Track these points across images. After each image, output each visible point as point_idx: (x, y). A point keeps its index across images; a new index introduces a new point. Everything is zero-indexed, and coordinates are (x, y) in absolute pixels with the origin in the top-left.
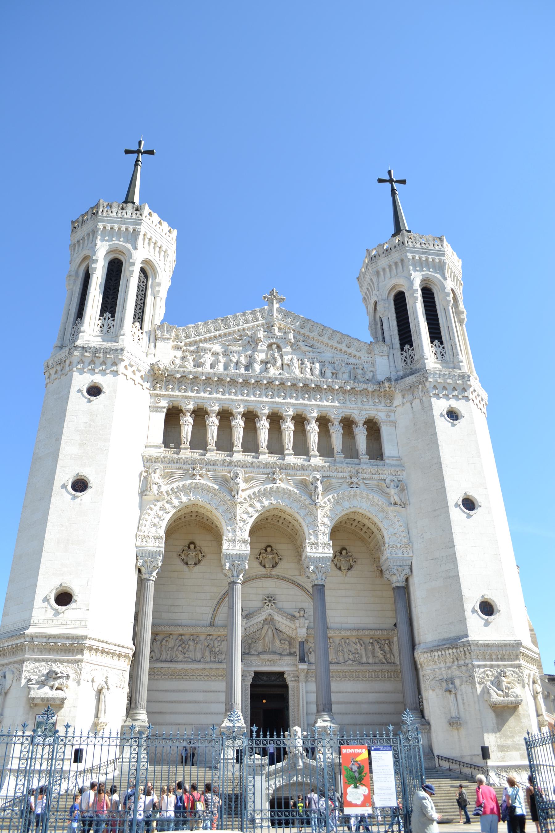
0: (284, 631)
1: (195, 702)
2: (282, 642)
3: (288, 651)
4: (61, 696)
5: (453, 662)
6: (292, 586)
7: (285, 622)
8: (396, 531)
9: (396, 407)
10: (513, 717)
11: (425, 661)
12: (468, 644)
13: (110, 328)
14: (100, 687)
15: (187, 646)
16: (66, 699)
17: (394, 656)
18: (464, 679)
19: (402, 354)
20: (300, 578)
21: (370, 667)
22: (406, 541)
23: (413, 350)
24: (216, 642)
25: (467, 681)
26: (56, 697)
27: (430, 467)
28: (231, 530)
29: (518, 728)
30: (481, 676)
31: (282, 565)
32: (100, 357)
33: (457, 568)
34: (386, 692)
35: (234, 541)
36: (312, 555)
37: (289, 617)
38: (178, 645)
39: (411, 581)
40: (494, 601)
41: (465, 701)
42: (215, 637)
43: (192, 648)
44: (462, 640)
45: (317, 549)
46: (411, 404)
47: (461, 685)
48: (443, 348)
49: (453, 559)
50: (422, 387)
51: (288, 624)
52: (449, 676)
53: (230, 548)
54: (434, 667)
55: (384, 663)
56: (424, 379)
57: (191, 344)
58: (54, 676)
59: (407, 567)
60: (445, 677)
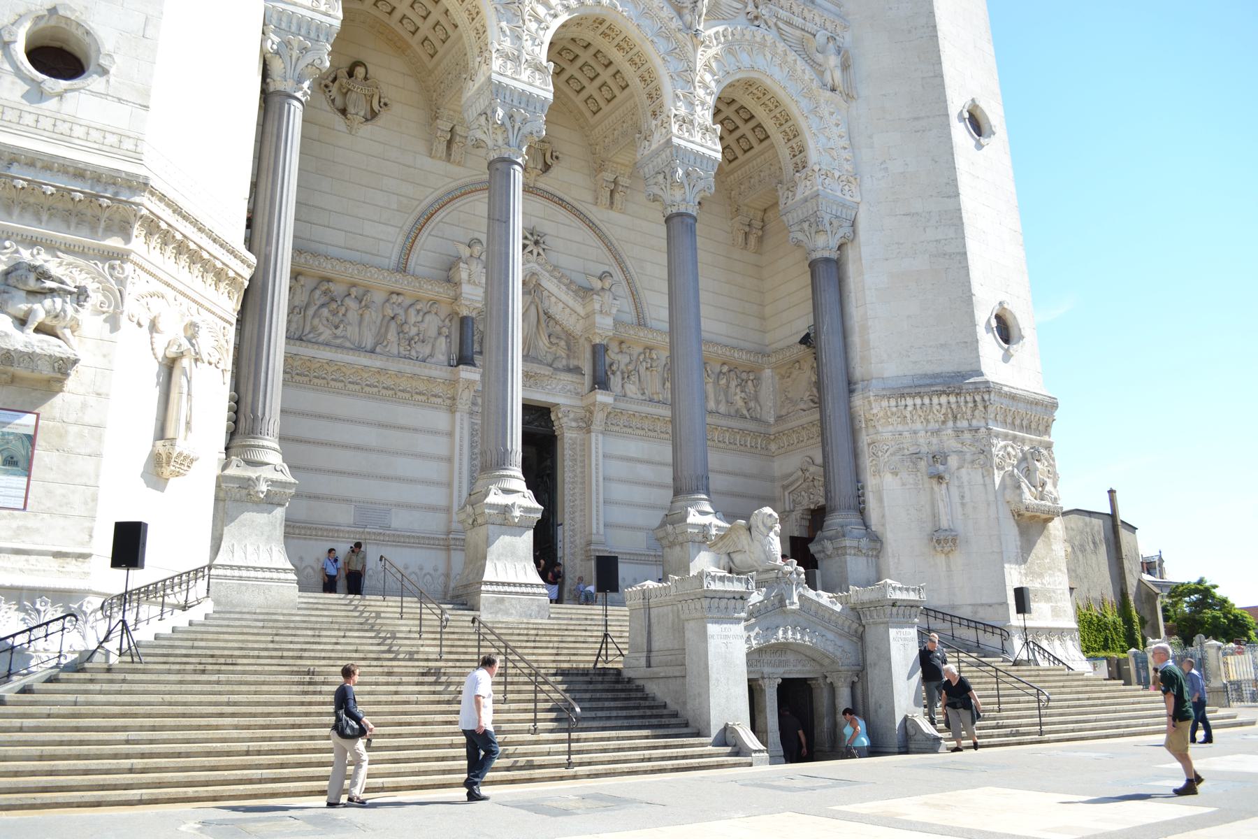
0: (558, 317)
1: (358, 448)
2: (554, 340)
3: (564, 362)
5: (944, 422)
6: (578, 222)
7: (564, 297)
10: (1042, 538)
11: (881, 414)
12: (988, 387)
14: (172, 352)
15: (343, 310)
16: (75, 362)
17: (760, 406)
18: (968, 457)
20: (594, 209)
21: (724, 422)
22: (850, 170)
24: (412, 311)
25: (973, 462)
26: (38, 351)
27: (910, 32)
28: (508, 32)
30: (1001, 453)
31: (556, 171)
33: (964, 238)
34: (745, 476)
35: (516, 59)
36: (683, 143)
37: (573, 287)
38: (318, 303)
39: (850, 253)
40: (1015, 318)
41: (967, 499)
42: (408, 302)
43: (353, 316)
44: (972, 380)
45: (691, 135)
47: (959, 468)
49: (955, 220)
51: (571, 302)
52: (934, 448)
53: (509, 73)
54: (900, 428)
55: (746, 418)
58: (32, 284)
59: (848, 224)
60: (924, 449)
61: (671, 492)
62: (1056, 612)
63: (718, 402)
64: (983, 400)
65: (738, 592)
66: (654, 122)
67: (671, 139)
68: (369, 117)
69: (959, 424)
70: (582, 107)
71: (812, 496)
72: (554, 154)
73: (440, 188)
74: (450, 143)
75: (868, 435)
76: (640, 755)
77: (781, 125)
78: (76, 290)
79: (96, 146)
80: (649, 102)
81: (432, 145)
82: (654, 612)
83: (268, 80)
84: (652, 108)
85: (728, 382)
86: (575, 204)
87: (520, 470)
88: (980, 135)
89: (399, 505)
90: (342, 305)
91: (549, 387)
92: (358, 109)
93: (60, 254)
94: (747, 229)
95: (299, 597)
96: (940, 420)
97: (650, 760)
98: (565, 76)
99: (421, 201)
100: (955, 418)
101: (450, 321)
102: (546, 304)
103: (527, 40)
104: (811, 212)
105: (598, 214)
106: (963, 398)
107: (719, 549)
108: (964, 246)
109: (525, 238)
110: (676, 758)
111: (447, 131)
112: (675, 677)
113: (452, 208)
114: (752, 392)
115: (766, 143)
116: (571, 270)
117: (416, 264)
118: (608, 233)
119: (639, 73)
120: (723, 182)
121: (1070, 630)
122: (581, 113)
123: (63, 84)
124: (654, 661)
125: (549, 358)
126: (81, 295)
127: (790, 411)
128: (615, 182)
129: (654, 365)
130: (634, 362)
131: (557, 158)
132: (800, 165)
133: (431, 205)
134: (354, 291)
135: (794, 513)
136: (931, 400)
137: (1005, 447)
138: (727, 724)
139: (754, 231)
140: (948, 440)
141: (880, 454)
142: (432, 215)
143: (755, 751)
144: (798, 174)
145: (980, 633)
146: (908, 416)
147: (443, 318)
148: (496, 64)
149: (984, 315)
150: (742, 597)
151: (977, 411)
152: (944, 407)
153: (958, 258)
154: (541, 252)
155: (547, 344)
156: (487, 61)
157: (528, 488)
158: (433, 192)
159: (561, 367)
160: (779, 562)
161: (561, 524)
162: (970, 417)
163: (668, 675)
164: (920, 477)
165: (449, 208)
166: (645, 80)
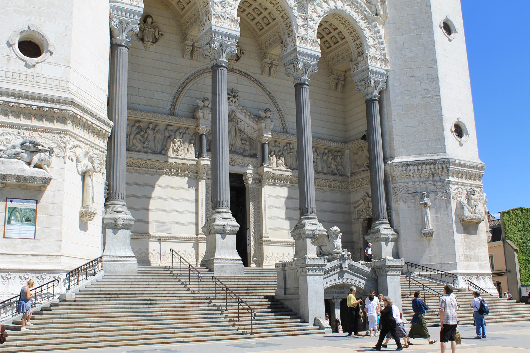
0: (245, 131)
2: (243, 142)
3: (249, 152)
6: (253, 84)
8: (375, 43)
14: (85, 169)
15: (146, 135)
16: (51, 179)
17: (344, 168)
26: (37, 176)
29: (478, 242)
30: (455, 192)
38: (135, 132)
39: (385, 95)
40: (465, 125)
42: (175, 129)
49: (435, 79)
53: (219, 25)
54: (408, 180)
55: (336, 175)
58: (33, 149)
61: (298, 212)
62: (481, 266)
63: (323, 168)
64: (447, 167)
65: (320, 264)
66: (288, 39)
67: (296, 48)
69: (435, 178)
70: (255, 27)
71: (368, 212)
72: (242, 51)
73: (188, 73)
74: (192, 52)
75: (393, 184)
76: (280, 329)
77: (351, 33)
78: (49, 149)
79: (50, 86)
81: (184, 52)
82: (287, 272)
83: (113, 39)
84: (287, 31)
85: (328, 157)
87: (229, 208)
89: (175, 223)
90: (146, 133)
91: (241, 165)
92: (149, 39)
93: (40, 133)
94: (337, 81)
95: (138, 268)
96: (426, 176)
97: (284, 331)
99: (180, 80)
102: (239, 124)
103: (227, 7)
104: (365, 77)
105: (263, 79)
106: (437, 166)
107: (316, 244)
108: (439, 92)
109: (229, 94)
110: (294, 331)
111: (190, 46)
112: (295, 299)
113: (194, 82)
114: (340, 162)
115: (344, 40)
116: (251, 108)
117: (179, 111)
118: (268, 88)
119: (281, 15)
120: (324, 58)
121: (488, 274)
122: (254, 29)
124: (287, 292)
125: (242, 151)
126: (51, 151)
127: (358, 171)
128: (271, 63)
130: (282, 151)
131: (243, 53)
132: (360, 53)
134: (151, 126)
135: (360, 220)
136: (422, 167)
137: (458, 188)
138: (316, 318)
140: (430, 186)
141: (398, 193)
142: (185, 86)
143: (326, 328)
144: (359, 57)
145: (443, 276)
146: (411, 175)
147: (191, 135)
148: (213, 21)
150: (322, 266)
151: (444, 172)
152: (428, 171)
153: (436, 97)
154: (236, 100)
155: (240, 143)
156: (210, 19)
157: (233, 217)
158: (185, 75)
159: (247, 154)
160: (341, 250)
161: (249, 229)
163: (292, 298)
164: (417, 204)
165: (193, 82)
166: (284, 18)
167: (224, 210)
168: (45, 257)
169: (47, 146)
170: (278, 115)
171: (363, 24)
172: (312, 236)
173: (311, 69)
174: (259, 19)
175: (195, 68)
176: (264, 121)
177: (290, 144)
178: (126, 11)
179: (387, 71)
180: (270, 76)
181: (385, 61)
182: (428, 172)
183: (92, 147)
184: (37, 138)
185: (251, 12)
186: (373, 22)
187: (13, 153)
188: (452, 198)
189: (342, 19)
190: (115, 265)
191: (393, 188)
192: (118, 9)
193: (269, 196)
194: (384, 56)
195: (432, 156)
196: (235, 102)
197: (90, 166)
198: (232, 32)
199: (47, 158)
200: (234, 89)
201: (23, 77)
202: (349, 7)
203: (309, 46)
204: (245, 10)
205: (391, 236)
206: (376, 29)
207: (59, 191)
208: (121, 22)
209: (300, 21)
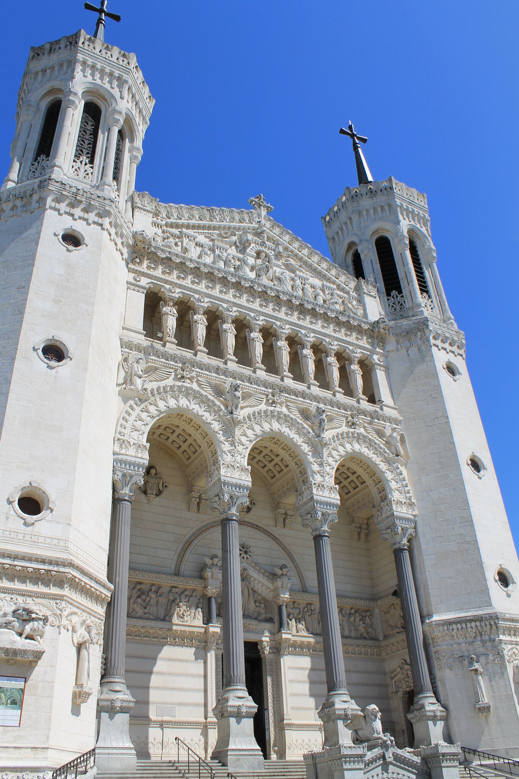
0: (259, 591)
2: (257, 604)
3: (264, 616)
4: (35, 649)
5: (475, 637)
6: (266, 538)
8: (399, 486)
9: (388, 352)
13: (87, 174)
14: (81, 640)
16: (43, 652)
19: (388, 300)
23: (402, 297)
26: (28, 648)
30: (509, 653)
32: (81, 202)
38: (136, 596)
39: (415, 543)
40: (509, 572)
42: (181, 591)
46: (407, 351)
48: (432, 302)
50: (421, 336)
53: (229, 475)
54: (451, 642)
56: (424, 327)
57: (171, 226)
58: (26, 617)
61: (325, 687)
63: (350, 631)
66: (304, 487)
68: (158, 494)
69: (483, 638)
70: (266, 474)
71: (407, 683)
74: (199, 504)
75: (434, 647)
78: (43, 618)
79: (49, 546)
80: (300, 475)
81: (190, 505)
83: (115, 493)
84: (302, 478)
85: (355, 619)
86: (265, 527)
88: (479, 471)
89: (180, 704)
90: (148, 596)
95: (137, 763)
96: (473, 636)
98: (256, 460)
99: (185, 536)
100: (481, 634)
101: (203, 599)
102: (252, 583)
104: (391, 524)
105: (277, 531)
106: (484, 623)
109: (240, 550)
114: (369, 623)
115: (364, 485)
117: (184, 570)
118: (283, 541)
119: (294, 461)
123: (35, 517)
125: (256, 614)
126: (45, 620)
128: (286, 514)
129: (313, 613)
130: (301, 613)
131: (254, 504)
133: (191, 537)
134: (154, 589)
135: (399, 693)
136: (466, 625)
137: (512, 649)
139: (363, 531)
140: (479, 647)
141: (441, 658)
142: (191, 542)
144: (382, 503)
146: (455, 635)
147: (199, 597)
148: (223, 471)
149: (491, 576)
156: (218, 469)
159: (262, 619)
161: (267, 709)
162: (489, 634)
164: (465, 671)
165: (200, 537)
167: (239, 687)
168: (30, 750)
169: (41, 614)
170: (295, 572)
171: (383, 467)
172: (343, 717)
173: (330, 518)
174: (270, 466)
175: (202, 522)
176: (281, 580)
177: (311, 604)
178: (130, 464)
179: (415, 516)
180: (285, 527)
181: (411, 505)
182: (474, 631)
183: (89, 613)
184: (31, 604)
185: (261, 460)
186: (394, 463)
187: (4, 622)
188: (507, 662)
189: (361, 462)
190: (110, 759)
191: (435, 653)
192: (121, 462)
193: (290, 668)
194: (410, 499)
195: (476, 611)
196: (247, 558)
197: (87, 637)
198: (242, 483)
199: (41, 627)
200: (246, 544)
201: (21, 536)
202: (367, 449)
203: (326, 493)
204: (254, 457)
205: (438, 714)
206: (398, 471)
207: (51, 666)
208: (124, 475)
209: (315, 467)
